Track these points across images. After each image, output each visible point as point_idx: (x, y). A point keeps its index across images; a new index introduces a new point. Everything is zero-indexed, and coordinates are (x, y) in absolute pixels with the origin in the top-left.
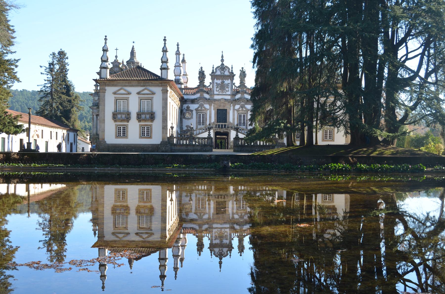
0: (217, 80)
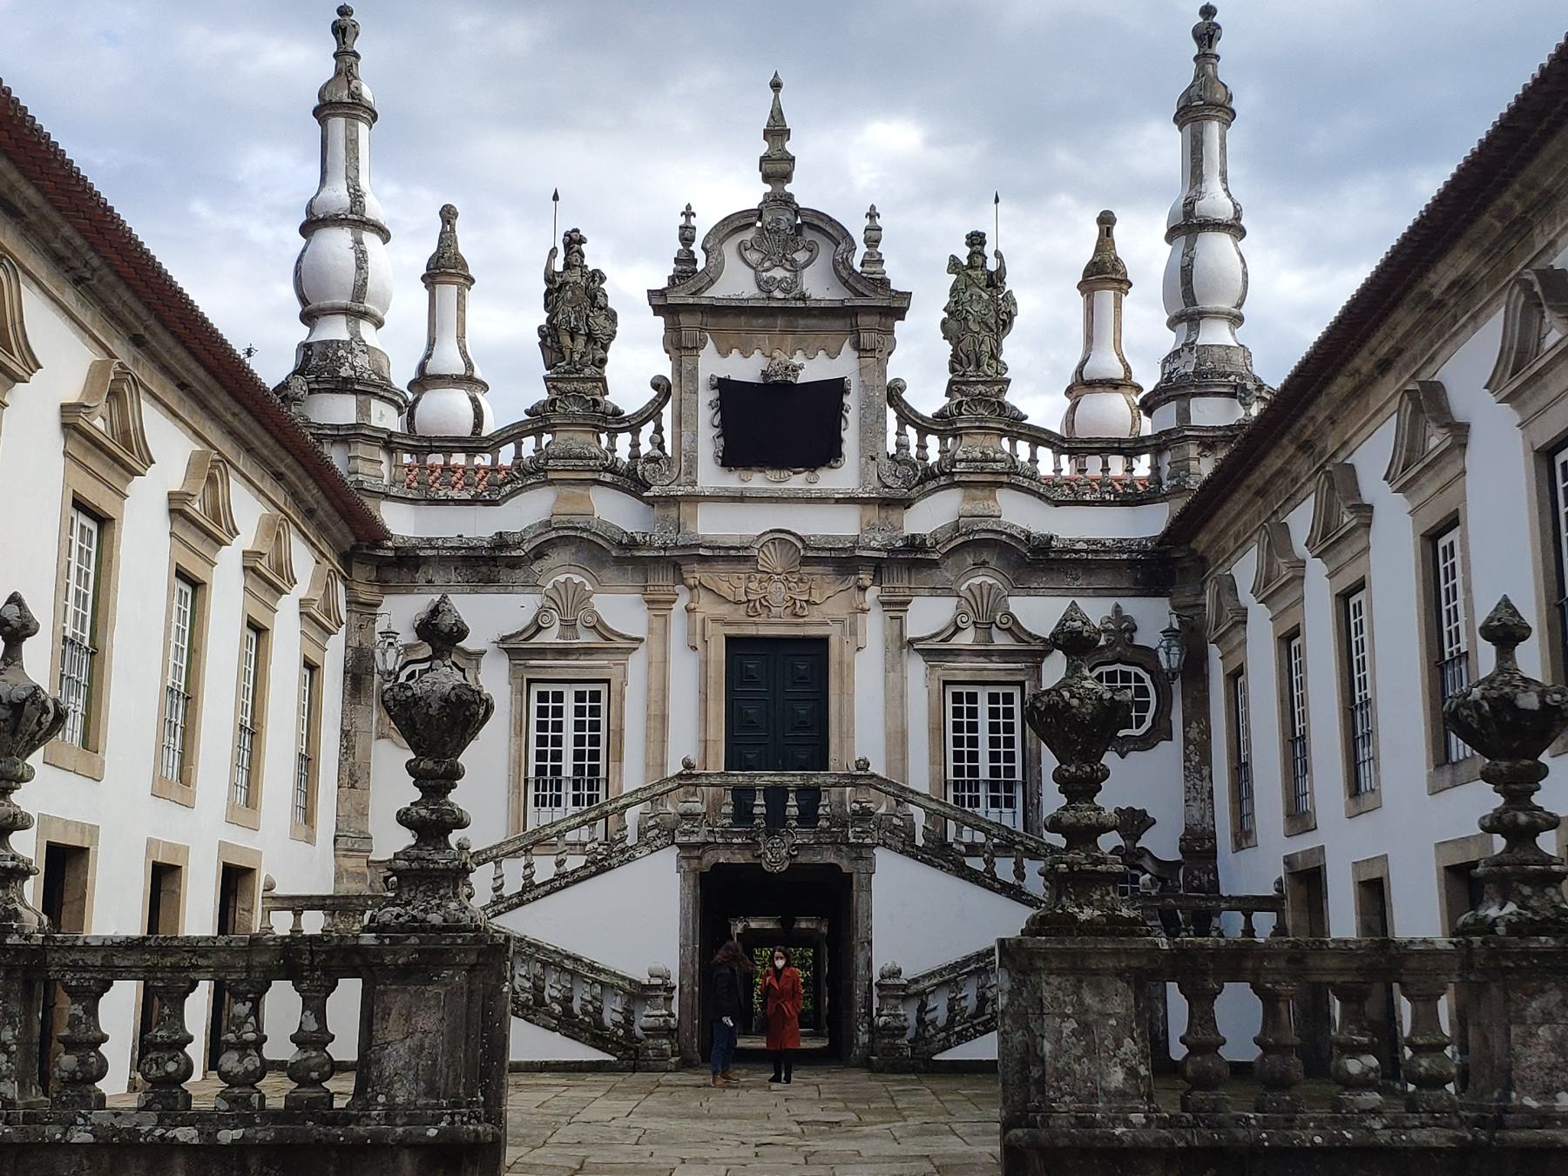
0: (724, 353)
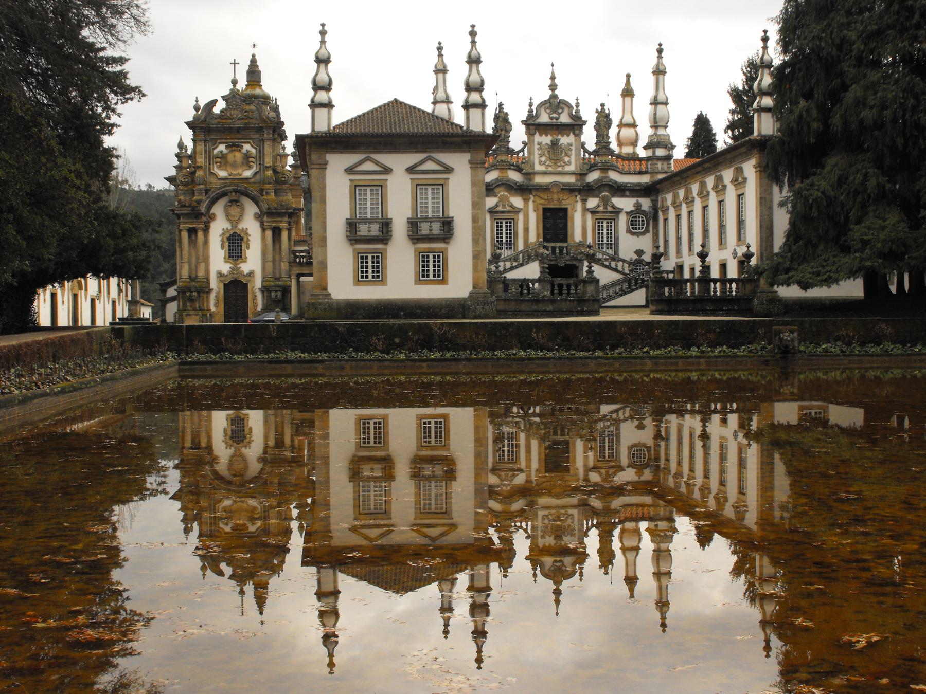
0: (541, 135)
